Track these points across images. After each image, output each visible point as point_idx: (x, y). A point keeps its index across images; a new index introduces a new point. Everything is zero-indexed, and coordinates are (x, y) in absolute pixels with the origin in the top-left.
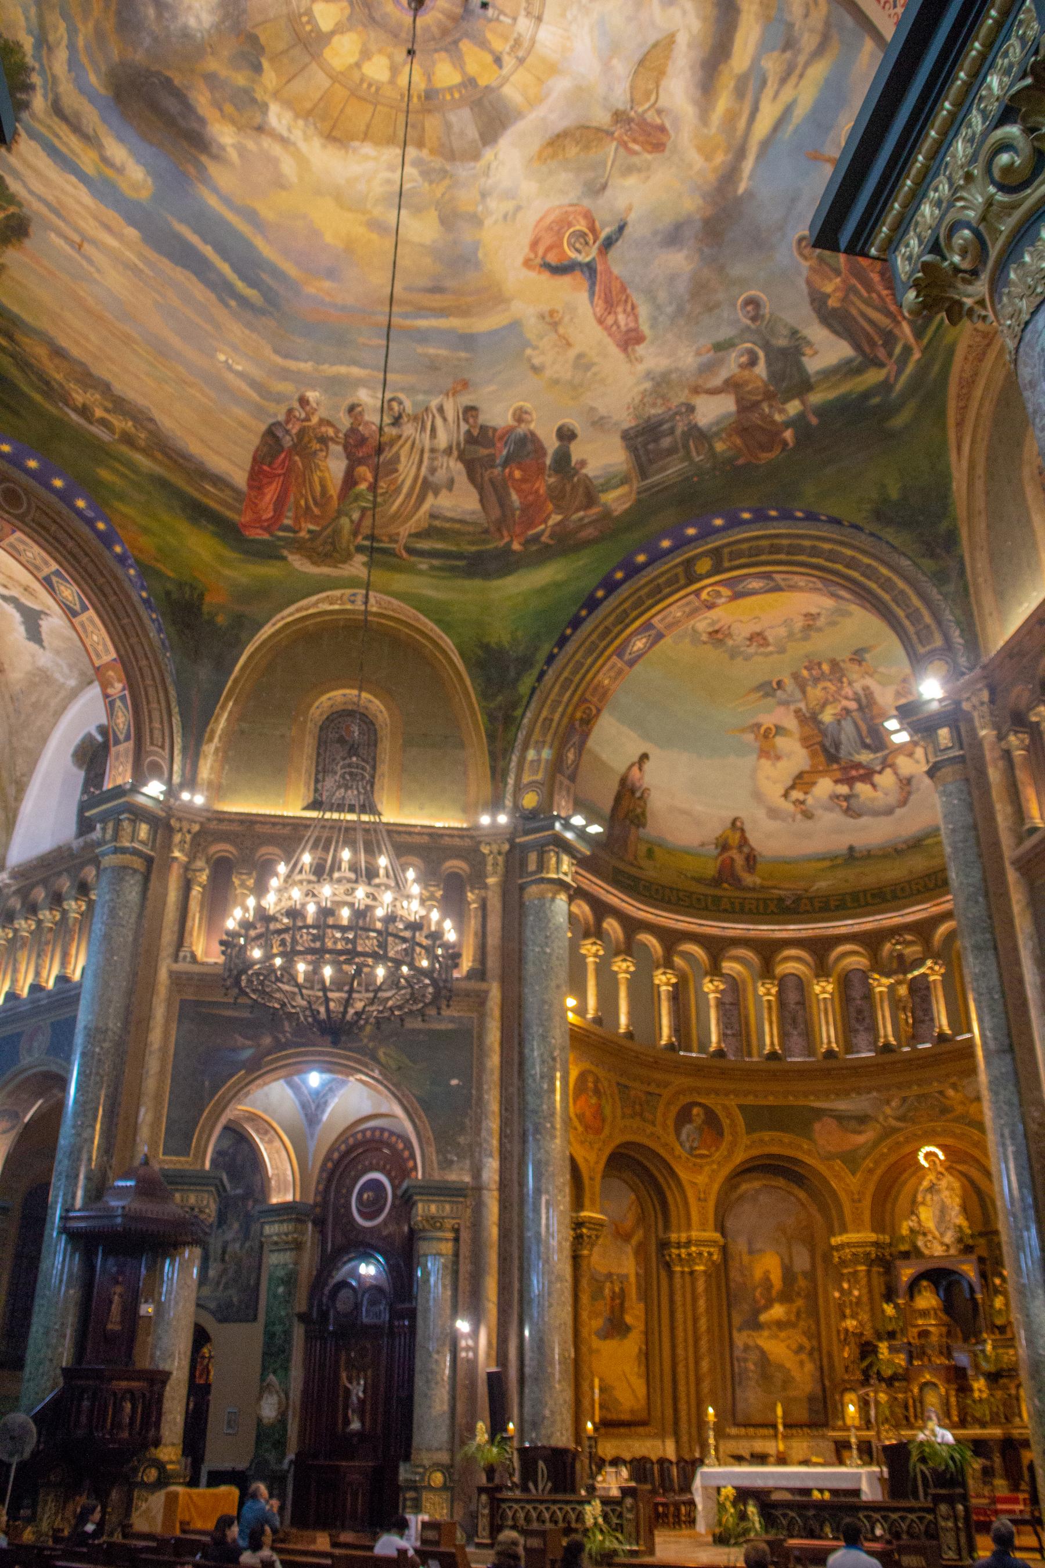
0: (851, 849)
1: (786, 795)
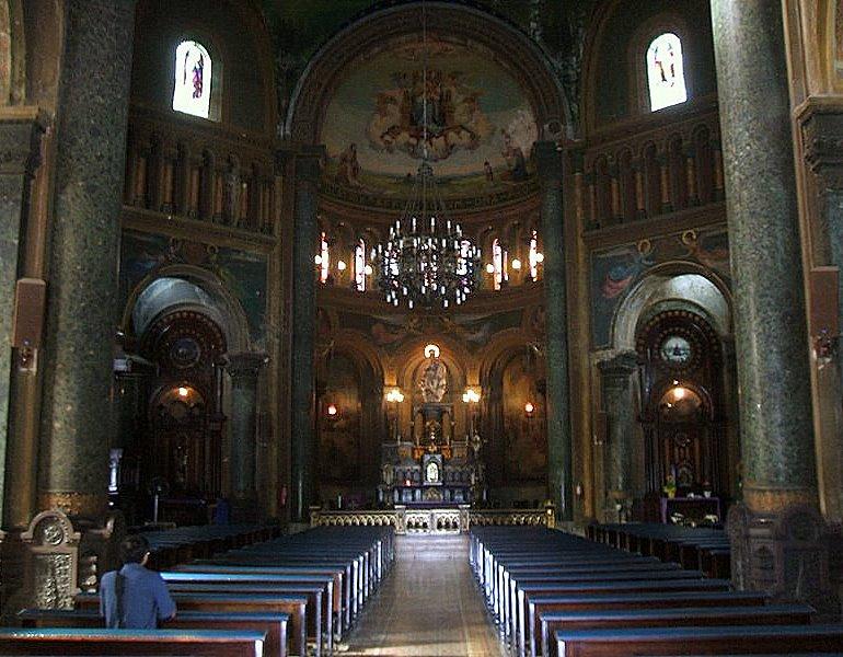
0: (409, 175)
1: (382, 137)
